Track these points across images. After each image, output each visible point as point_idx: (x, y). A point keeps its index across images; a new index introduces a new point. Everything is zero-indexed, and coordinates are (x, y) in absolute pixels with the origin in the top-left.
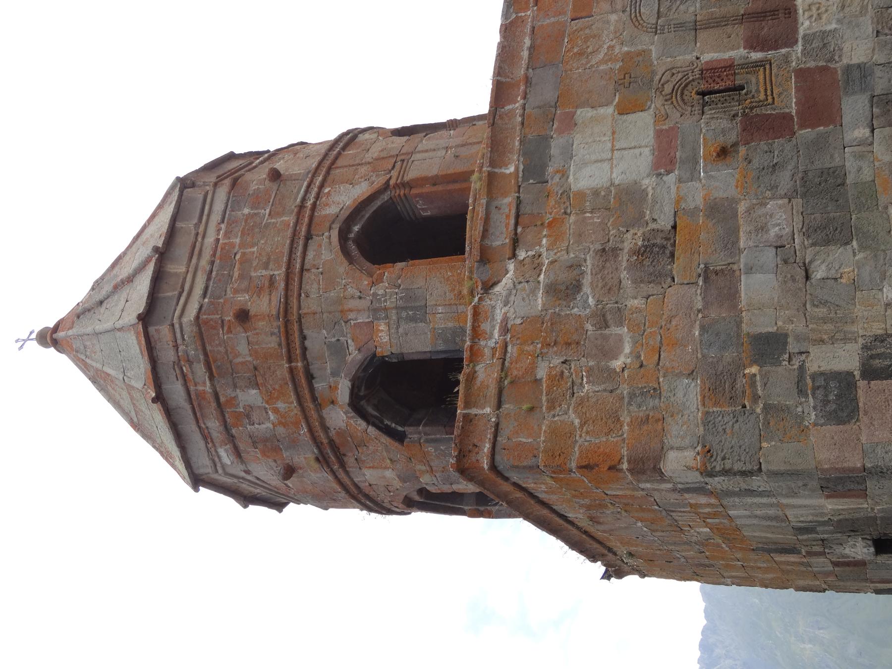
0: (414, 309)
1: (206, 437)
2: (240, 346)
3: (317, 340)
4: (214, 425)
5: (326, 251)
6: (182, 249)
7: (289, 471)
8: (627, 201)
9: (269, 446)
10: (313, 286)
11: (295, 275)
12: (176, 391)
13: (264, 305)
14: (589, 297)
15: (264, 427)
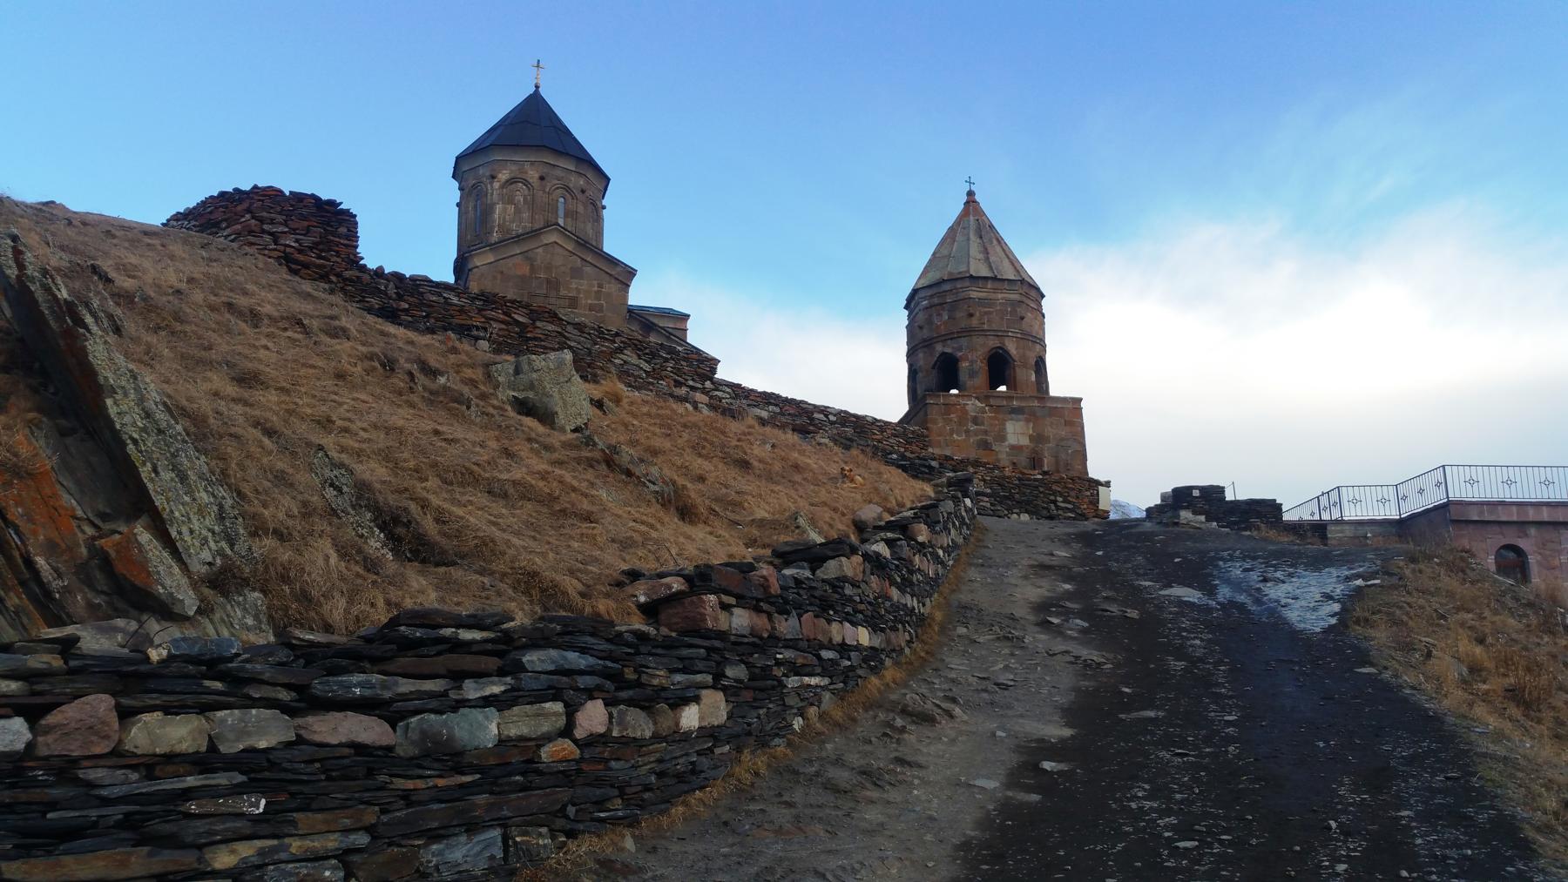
0: (972, 374)
1: (932, 296)
2: (959, 314)
3: (964, 342)
4: (936, 300)
5: (993, 342)
6: (997, 285)
7: (921, 328)
8: (1002, 437)
9: (929, 321)
10: (981, 340)
11: (983, 333)
12: (947, 287)
13: (974, 322)
14: (973, 428)
15: (936, 321)
